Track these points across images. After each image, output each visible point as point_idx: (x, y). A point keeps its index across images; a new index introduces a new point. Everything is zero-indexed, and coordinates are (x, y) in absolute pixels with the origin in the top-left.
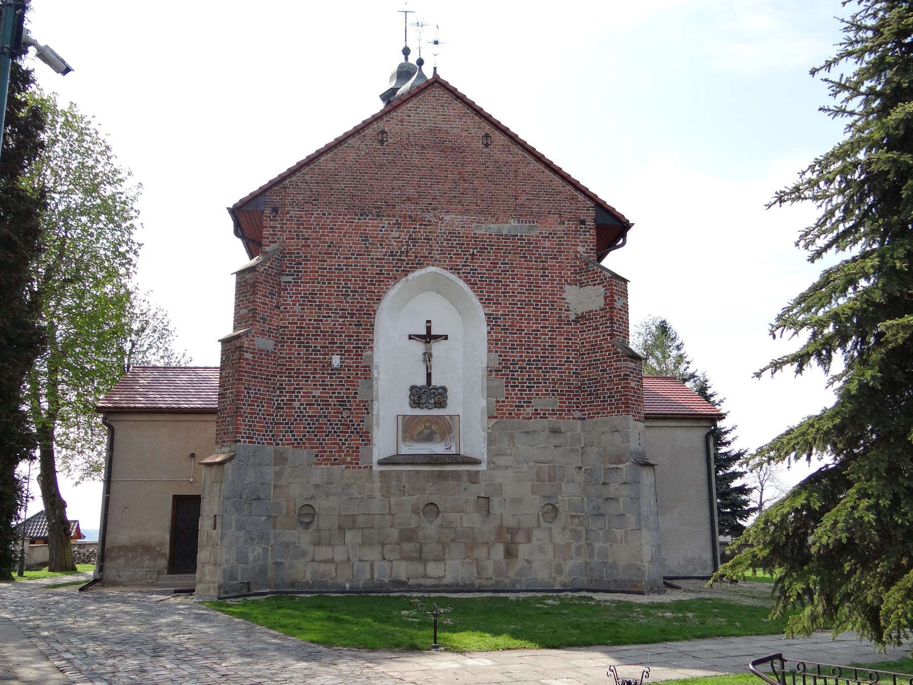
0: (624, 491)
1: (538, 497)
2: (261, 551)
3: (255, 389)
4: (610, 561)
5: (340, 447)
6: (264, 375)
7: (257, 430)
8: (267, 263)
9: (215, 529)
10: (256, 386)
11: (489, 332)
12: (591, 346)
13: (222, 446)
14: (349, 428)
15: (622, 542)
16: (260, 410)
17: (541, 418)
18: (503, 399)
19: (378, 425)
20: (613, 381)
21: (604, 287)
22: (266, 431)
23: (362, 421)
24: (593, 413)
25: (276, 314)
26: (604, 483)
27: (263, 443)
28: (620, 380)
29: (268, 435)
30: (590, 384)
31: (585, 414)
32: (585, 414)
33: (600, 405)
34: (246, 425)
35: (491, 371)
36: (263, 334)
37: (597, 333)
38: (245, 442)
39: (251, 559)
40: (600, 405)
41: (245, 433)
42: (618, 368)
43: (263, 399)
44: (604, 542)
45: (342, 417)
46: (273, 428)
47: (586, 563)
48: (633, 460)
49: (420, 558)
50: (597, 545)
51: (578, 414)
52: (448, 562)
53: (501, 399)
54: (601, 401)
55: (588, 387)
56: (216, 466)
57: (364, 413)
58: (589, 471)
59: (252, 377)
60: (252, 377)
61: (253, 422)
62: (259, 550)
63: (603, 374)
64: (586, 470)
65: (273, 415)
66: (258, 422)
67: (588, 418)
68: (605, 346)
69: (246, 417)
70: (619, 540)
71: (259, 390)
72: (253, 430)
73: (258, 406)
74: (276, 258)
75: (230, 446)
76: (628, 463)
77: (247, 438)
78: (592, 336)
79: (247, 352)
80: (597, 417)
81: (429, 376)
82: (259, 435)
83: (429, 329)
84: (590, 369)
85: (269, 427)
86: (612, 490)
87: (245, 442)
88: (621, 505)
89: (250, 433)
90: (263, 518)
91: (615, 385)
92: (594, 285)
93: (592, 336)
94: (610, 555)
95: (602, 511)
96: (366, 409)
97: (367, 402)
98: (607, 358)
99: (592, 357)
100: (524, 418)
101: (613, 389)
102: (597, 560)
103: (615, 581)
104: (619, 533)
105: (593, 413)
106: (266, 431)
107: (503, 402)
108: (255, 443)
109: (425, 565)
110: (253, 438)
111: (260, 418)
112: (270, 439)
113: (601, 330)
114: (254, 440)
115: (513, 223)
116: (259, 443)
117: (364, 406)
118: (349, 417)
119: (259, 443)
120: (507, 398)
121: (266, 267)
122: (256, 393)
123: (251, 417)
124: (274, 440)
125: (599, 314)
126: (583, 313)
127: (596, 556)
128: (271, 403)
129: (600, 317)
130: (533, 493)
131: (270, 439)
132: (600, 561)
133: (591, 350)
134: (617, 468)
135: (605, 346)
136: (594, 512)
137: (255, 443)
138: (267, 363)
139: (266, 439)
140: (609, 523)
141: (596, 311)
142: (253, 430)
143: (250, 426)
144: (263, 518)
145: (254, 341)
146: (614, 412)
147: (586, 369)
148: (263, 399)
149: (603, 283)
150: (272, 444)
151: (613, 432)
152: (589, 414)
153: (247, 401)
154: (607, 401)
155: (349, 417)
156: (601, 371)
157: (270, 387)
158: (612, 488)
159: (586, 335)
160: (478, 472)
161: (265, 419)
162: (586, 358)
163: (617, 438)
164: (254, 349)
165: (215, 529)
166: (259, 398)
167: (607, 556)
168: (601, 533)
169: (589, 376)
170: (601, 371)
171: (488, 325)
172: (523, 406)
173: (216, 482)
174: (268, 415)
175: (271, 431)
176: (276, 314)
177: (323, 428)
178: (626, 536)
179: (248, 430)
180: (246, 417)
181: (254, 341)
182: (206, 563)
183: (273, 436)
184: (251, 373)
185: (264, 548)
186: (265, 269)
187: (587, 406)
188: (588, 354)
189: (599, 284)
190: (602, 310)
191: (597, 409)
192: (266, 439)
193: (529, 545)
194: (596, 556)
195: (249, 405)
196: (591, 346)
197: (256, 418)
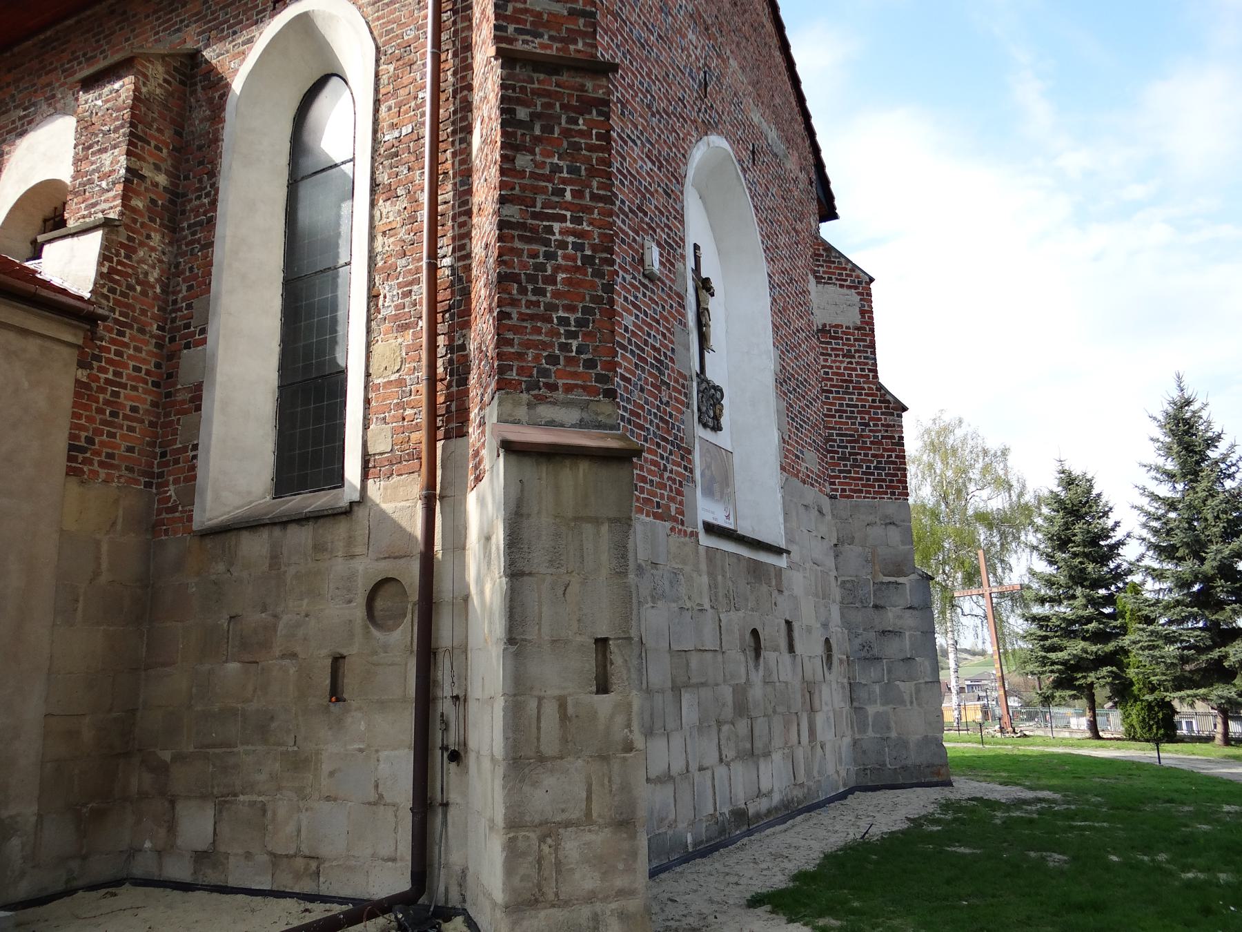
0: (910, 621)
4: (894, 735)
5: (661, 477)
9: (603, 687)
12: (842, 381)
13: (541, 399)
14: (668, 432)
15: (912, 703)
20: (881, 443)
21: (859, 294)
23: (683, 423)
24: (851, 490)
26: (876, 607)
28: (893, 444)
30: (842, 441)
31: (836, 490)
32: (836, 490)
33: (861, 479)
37: (851, 363)
40: (861, 479)
42: (889, 426)
44: (883, 704)
45: (661, 402)
47: (855, 743)
48: (921, 573)
50: (871, 710)
51: (828, 488)
54: (864, 473)
55: (839, 447)
56: (584, 467)
57: (682, 403)
58: (848, 585)
63: (863, 430)
64: (844, 582)
67: (841, 496)
68: (866, 386)
70: (907, 698)
75: (584, 406)
76: (913, 577)
78: (843, 366)
80: (857, 497)
84: (840, 417)
86: (891, 617)
88: (907, 642)
91: (885, 450)
92: (842, 286)
93: (843, 366)
94: (893, 724)
95: (875, 651)
96: (686, 395)
97: (685, 378)
98: (870, 407)
99: (844, 399)
101: (883, 456)
102: (873, 735)
103: (905, 768)
104: (906, 688)
105: (851, 490)
113: (857, 360)
117: (683, 386)
118: (667, 404)
125: (853, 334)
126: (825, 325)
127: (870, 728)
129: (855, 340)
132: (879, 736)
133: (842, 387)
134: (896, 583)
135: (866, 386)
136: (863, 654)
140: (889, 672)
141: (848, 328)
146: (886, 493)
147: (834, 416)
149: (856, 288)
151: (886, 524)
152: (844, 490)
154: (873, 474)
155: (667, 404)
156: (860, 424)
158: (890, 615)
159: (834, 362)
162: (834, 398)
163: (894, 535)
165: (603, 687)
167: (888, 728)
168: (877, 688)
169: (840, 429)
170: (860, 424)
173: (596, 521)
177: (638, 416)
178: (918, 691)
182: (567, 824)
187: (839, 477)
188: (838, 392)
189: (849, 287)
190: (858, 329)
191: (857, 485)
194: (870, 728)
196: (842, 381)
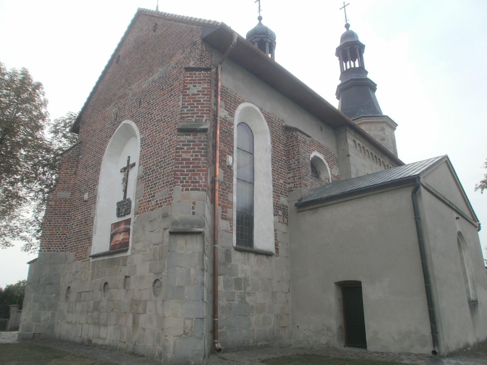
1: (152, 274)
2: (50, 315)
3: (55, 221)
6: (62, 212)
7: (54, 244)
8: (70, 151)
10: (56, 219)
11: (141, 151)
16: (57, 232)
17: (159, 207)
18: (142, 198)
19: (95, 233)
22: (61, 244)
25: (73, 178)
27: (58, 251)
29: (62, 246)
34: (46, 242)
35: (139, 179)
36: (63, 190)
38: (45, 251)
39: (43, 318)
41: (46, 246)
43: (60, 226)
46: (66, 242)
49: (97, 324)
52: (109, 327)
53: (141, 199)
59: (54, 214)
60: (54, 214)
61: (52, 239)
62: (49, 314)
65: (66, 234)
66: (55, 239)
69: (47, 237)
71: (58, 221)
72: (51, 244)
73: (56, 230)
74: (76, 148)
77: (47, 248)
79: (51, 201)
81: (125, 191)
82: (55, 246)
83: (129, 161)
85: (62, 241)
87: (45, 251)
89: (49, 246)
90: (54, 295)
100: (151, 210)
106: (61, 244)
107: (142, 200)
108: (52, 251)
109: (100, 329)
110: (50, 248)
111: (57, 237)
112: (63, 248)
114: (51, 250)
115: (161, 70)
116: (54, 251)
119: (54, 251)
120: (144, 197)
121: (70, 154)
122: (56, 223)
123: (51, 237)
124: (65, 249)
128: (65, 228)
130: (150, 271)
131: (63, 248)
137: (52, 251)
138: (64, 205)
139: (60, 249)
142: (51, 244)
143: (49, 242)
144: (54, 295)
145: (56, 194)
148: (60, 226)
150: (64, 251)
153: (48, 228)
157: (66, 219)
160: (127, 257)
161: (60, 237)
164: (57, 199)
166: (57, 225)
171: (141, 146)
172: (150, 201)
174: (62, 234)
175: (64, 244)
176: (73, 178)
179: (48, 244)
180: (47, 237)
181: (56, 194)
183: (65, 246)
184: (53, 212)
185: (52, 313)
186: (69, 155)
192: (60, 249)
193: (144, 315)
195: (50, 230)
197: (54, 237)
